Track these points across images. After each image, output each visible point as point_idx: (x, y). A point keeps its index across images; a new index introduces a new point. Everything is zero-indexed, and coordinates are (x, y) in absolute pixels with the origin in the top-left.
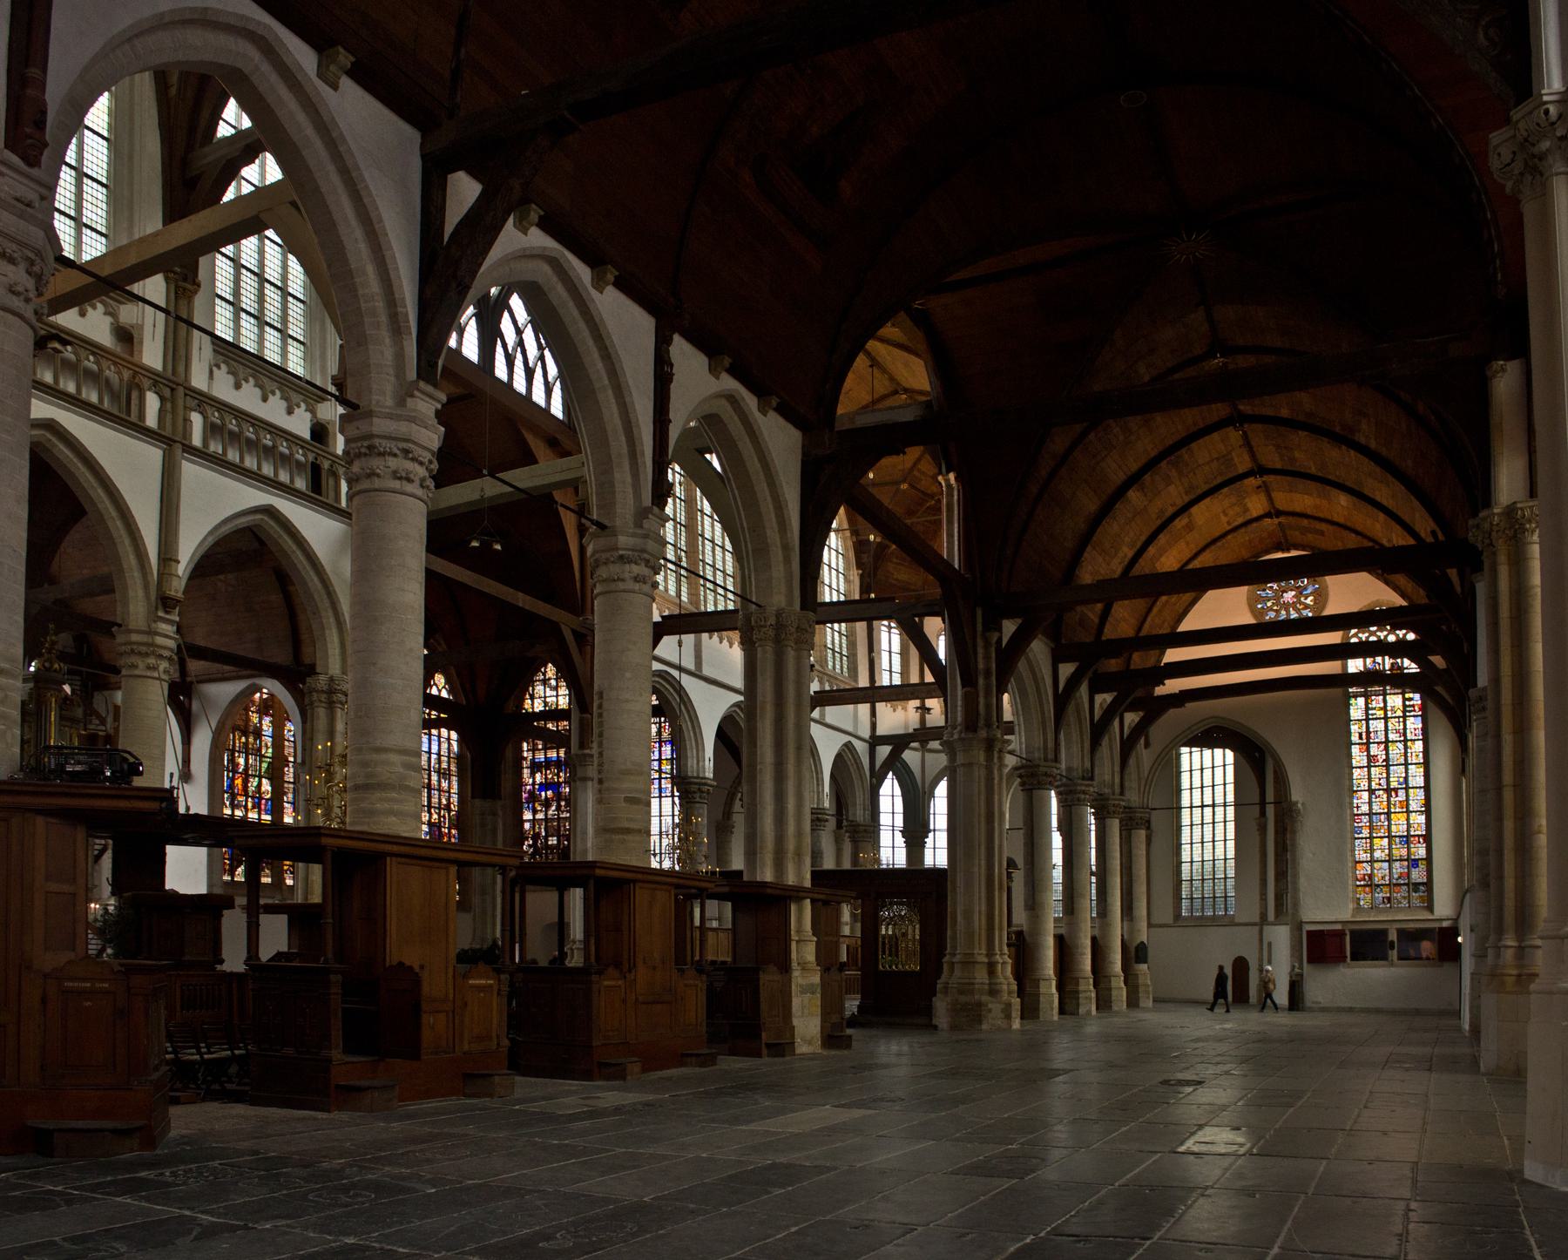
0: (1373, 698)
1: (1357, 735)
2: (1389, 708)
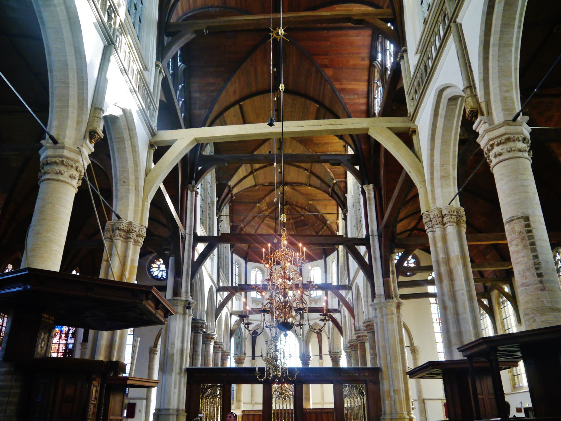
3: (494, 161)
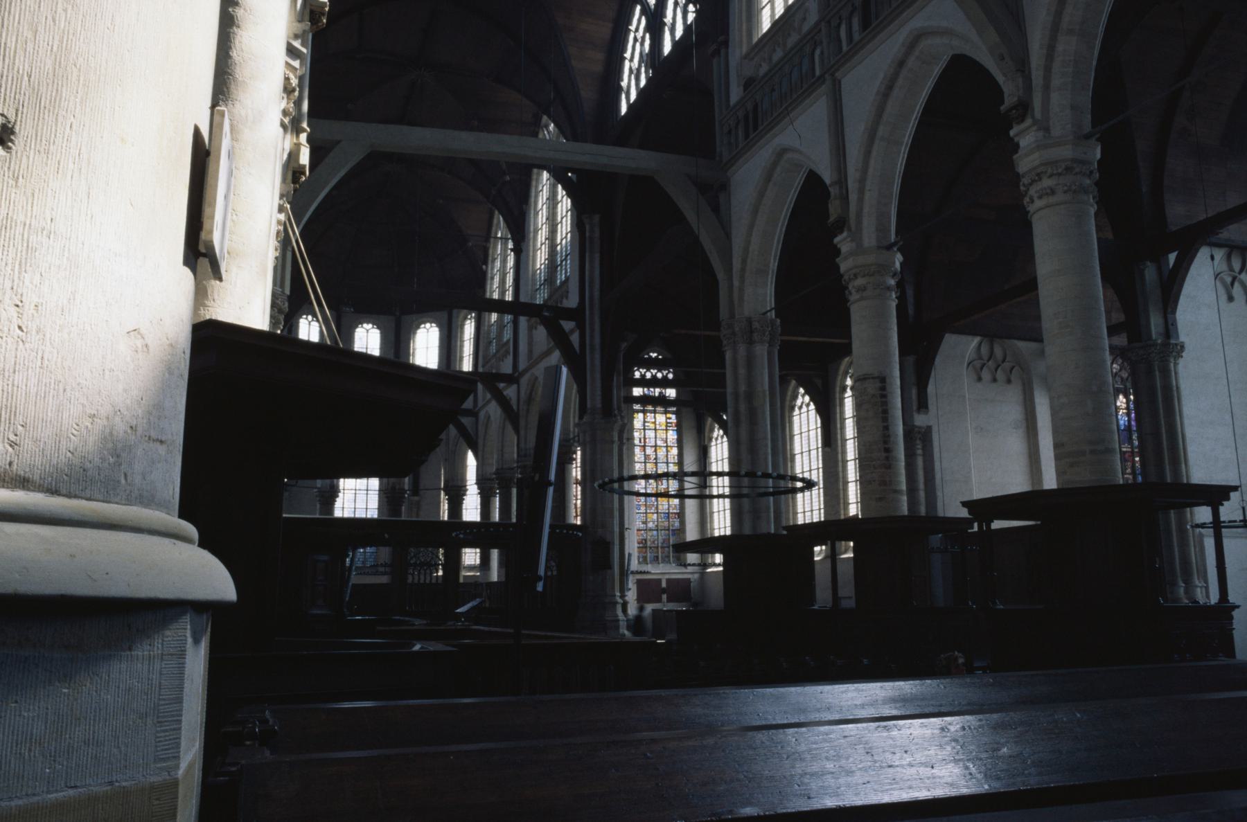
0: (648, 414)
3: (854, 297)
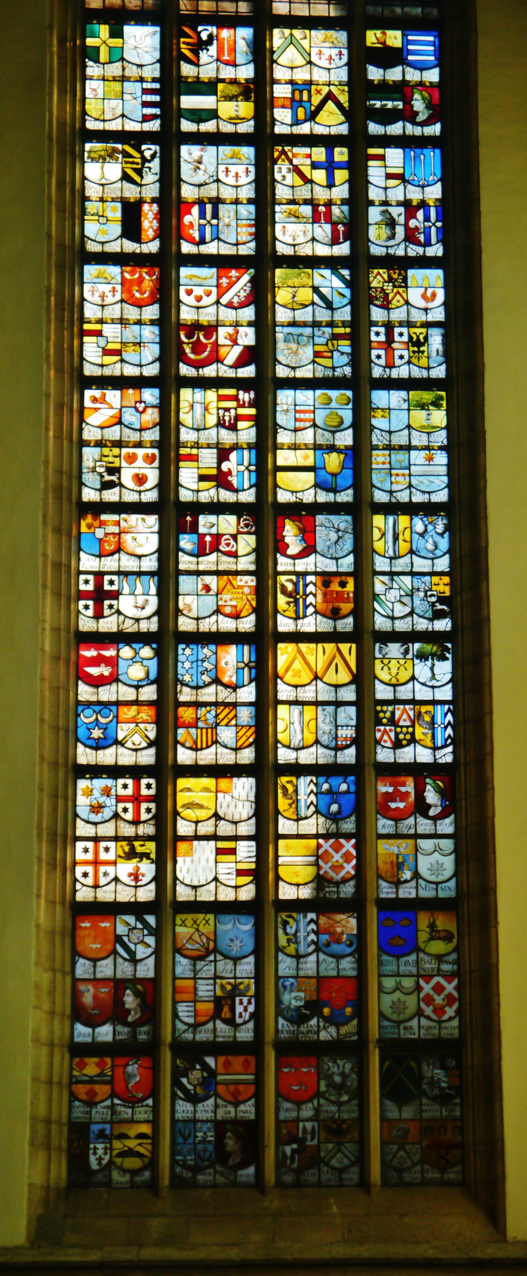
1: (115, 212)
2: (281, 91)
